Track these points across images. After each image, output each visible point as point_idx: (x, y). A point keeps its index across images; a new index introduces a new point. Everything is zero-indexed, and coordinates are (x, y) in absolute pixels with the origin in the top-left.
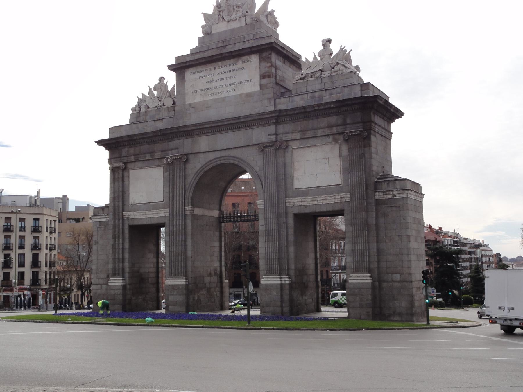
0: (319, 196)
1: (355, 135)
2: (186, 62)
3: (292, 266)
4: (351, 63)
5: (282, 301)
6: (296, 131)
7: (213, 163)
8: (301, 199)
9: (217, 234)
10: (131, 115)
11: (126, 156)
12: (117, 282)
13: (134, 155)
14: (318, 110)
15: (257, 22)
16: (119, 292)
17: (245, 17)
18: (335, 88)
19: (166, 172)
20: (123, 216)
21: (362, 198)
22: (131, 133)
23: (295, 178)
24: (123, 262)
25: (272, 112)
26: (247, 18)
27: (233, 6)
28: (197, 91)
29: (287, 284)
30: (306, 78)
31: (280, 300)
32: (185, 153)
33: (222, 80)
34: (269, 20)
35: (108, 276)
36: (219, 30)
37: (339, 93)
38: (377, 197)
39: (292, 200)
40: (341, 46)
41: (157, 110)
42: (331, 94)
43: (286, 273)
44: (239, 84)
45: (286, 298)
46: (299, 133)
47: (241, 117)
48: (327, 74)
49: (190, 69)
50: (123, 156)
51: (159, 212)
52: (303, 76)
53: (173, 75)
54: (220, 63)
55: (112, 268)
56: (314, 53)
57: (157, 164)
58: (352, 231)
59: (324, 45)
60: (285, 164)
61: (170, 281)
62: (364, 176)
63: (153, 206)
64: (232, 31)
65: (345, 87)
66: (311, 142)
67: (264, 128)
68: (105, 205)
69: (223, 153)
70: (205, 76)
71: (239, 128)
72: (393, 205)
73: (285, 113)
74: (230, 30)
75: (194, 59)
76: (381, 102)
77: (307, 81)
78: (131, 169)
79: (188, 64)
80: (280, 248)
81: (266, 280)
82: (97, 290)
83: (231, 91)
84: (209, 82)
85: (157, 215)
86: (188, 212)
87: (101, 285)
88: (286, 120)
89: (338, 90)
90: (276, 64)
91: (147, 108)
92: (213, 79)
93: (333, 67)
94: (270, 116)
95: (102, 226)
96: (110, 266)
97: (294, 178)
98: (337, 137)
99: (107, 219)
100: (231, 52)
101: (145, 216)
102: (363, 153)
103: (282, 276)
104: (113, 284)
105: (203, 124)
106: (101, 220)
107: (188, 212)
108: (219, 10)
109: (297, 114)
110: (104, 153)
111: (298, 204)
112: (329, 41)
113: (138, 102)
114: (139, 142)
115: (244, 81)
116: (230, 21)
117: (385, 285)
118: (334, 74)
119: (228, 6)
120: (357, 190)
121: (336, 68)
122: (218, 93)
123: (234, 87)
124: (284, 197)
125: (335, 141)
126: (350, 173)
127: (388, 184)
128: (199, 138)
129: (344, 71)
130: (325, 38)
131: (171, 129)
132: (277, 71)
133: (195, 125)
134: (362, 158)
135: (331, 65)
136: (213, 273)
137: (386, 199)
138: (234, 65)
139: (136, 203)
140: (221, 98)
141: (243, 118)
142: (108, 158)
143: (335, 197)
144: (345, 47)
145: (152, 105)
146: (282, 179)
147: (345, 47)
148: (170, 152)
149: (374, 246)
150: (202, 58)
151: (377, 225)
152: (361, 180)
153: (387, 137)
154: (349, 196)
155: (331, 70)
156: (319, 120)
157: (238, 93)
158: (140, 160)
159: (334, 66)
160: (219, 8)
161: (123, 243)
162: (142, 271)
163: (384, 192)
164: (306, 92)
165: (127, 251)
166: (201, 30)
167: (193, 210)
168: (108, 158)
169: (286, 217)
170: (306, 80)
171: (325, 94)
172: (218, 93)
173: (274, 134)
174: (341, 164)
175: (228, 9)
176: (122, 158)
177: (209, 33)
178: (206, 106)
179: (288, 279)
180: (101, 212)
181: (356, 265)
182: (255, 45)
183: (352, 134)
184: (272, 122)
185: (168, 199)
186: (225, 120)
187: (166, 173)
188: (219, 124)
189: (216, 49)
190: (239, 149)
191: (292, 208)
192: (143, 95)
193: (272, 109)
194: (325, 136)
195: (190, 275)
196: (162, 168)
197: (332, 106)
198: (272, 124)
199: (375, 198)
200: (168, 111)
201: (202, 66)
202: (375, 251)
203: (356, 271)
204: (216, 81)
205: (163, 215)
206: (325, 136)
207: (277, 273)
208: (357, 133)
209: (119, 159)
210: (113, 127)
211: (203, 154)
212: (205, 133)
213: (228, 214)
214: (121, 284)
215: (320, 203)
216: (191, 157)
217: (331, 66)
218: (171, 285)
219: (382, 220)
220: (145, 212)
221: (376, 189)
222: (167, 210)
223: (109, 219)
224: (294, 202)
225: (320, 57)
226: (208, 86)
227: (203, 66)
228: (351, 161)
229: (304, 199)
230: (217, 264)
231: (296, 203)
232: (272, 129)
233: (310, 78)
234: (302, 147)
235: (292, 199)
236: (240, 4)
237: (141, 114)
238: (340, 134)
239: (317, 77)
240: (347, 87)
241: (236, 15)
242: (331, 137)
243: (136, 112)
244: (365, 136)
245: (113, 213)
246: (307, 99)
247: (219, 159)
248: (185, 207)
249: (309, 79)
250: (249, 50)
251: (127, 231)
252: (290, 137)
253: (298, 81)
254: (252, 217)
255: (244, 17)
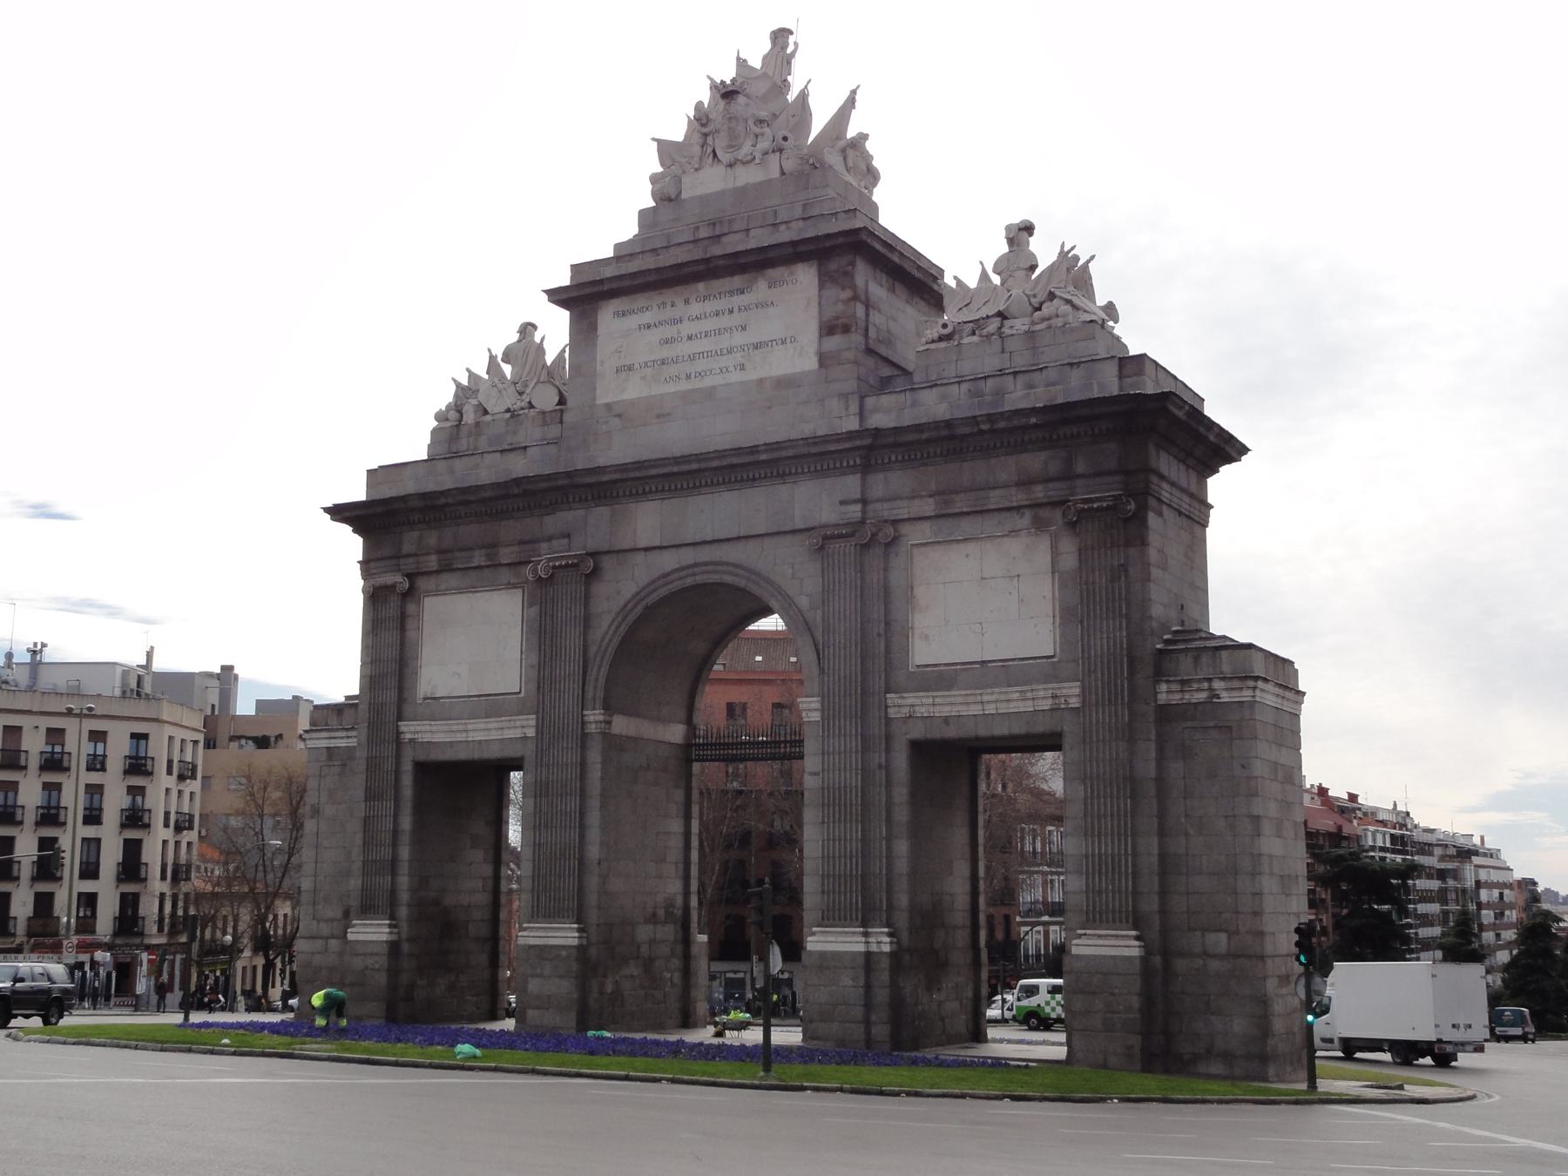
0: (989, 691)
1: (1098, 509)
2: (601, 282)
3: (903, 900)
4: (1090, 295)
5: (868, 1006)
6: (923, 493)
7: (671, 583)
8: (934, 697)
9: (679, 795)
10: (434, 432)
11: (416, 555)
12: (372, 932)
13: (439, 552)
14: (992, 431)
15: (816, 168)
16: (376, 962)
17: (781, 153)
18: (1041, 369)
19: (530, 606)
20: (399, 733)
21: (1116, 698)
22: (431, 486)
23: (917, 632)
24: (394, 872)
25: (851, 435)
26: (784, 156)
27: (746, 121)
28: (630, 368)
29: (886, 953)
30: (956, 337)
31: (862, 1003)
32: (590, 551)
34: (850, 164)
35: (347, 914)
36: (700, 191)
37: (1053, 384)
38: (1163, 698)
39: (904, 698)
40: (1063, 246)
41: (512, 420)
42: (1030, 386)
43: (881, 921)
44: (757, 348)
45: (882, 995)
46: (931, 501)
47: (761, 448)
48: (1019, 325)
49: (612, 301)
50: (404, 552)
51: (508, 724)
52: (946, 332)
53: (563, 316)
54: (701, 286)
55: (360, 888)
56: (981, 263)
57: (506, 582)
58: (1085, 799)
59: (1011, 241)
60: (887, 591)
61: (532, 934)
62: (1125, 634)
63: (490, 706)
64: (742, 191)
65: (1071, 365)
66: (967, 526)
67: (828, 482)
68: (347, 698)
69: (704, 554)
70: (657, 324)
71: (754, 479)
72: (1212, 724)
73: (891, 440)
74: (736, 190)
75: (624, 272)
76: (1180, 414)
77: (959, 344)
78: (429, 593)
79: (606, 288)
80: (865, 840)
81: (822, 939)
82: (313, 953)
84: (667, 342)
85: (500, 732)
86: (593, 726)
87: (327, 938)
88: (893, 459)
89: (1051, 374)
90: (867, 291)
91: (481, 412)
92: (679, 332)
93: (1037, 305)
94: (847, 445)
95: (336, 763)
96: (355, 883)
97: (913, 634)
98: (1045, 513)
99: (350, 740)
100: (737, 254)
101: (464, 735)
102: (1122, 565)
103: (870, 930)
104: (361, 937)
105: (646, 464)
106: (333, 743)
107: (593, 726)
108: (705, 130)
109: (928, 441)
110: (351, 544)
111: (922, 711)
112: (1028, 229)
113: (456, 396)
114: (453, 515)
115: (772, 341)
116: (735, 163)
117: (1180, 964)
118: (1038, 327)
119: (730, 118)
120: (1103, 674)
121: (1047, 309)
122: (693, 374)
123: (742, 357)
124: (883, 689)
125: (1039, 525)
126: (1081, 622)
127: (1196, 659)
128: (633, 505)
129: (1070, 319)
130: (1016, 220)
131: (549, 477)
132: (871, 312)
133: (623, 468)
134: (1120, 578)
135: (1033, 300)
136: (661, 912)
137: (1189, 704)
138: (742, 293)
139: (437, 696)
140: (701, 390)
141: (766, 451)
142: (361, 559)
143: (1035, 693)
144: (1073, 248)
145: (496, 406)
146: (879, 635)
147: (1073, 248)
148: (544, 546)
149: (1150, 846)
150: (649, 270)
151: (1160, 781)
152: (1115, 642)
153: (1197, 519)
154: (1077, 691)
155: (1033, 313)
156: (993, 461)
157: (752, 375)
158: (455, 566)
159: (1041, 304)
160: (703, 125)
161: (396, 816)
162: (449, 901)
163: (1183, 682)
164: (957, 377)
165: (405, 838)
166: (649, 187)
167: (609, 723)
168: (361, 559)
169: (888, 751)
170: (956, 343)
171: (1013, 387)
172: (693, 374)
173: (855, 502)
174: (1057, 595)
175: (730, 128)
176: (402, 561)
177: (673, 197)
178: (658, 411)
179: (888, 940)
180: (334, 722)
181: (1094, 901)
182: (810, 234)
183: (1090, 505)
184: (852, 463)
185: (533, 686)
186: (712, 455)
187: (532, 609)
188: (694, 466)
189: (691, 246)
190: (751, 542)
191: (905, 722)
192: (471, 375)
193: (852, 424)
194: (1009, 509)
195: (593, 916)
196: (519, 592)
197: (1033, 420)
198: (851, 470)
199: (1156, 700)
200: (545, 424)
201: (646, 295)
202: (1155, 860)
203: (1094, 921)
204: (690, 338)
205: (518, 733)
206: (1009, 509)
207: (857, 919)
208: (1105, 505)
209: (394, 562)
210: (380, 467)
211: (642, 554)
212: (650, 492)
213: (712, 737)
214: (385, 939)
215: (991, 709)
216: (607, 563)
217: (1030, 304)
218: (536, 946)
219: (1176, 768)
220: (466, 724)
221: (1159, 674)
222: (531, 720)
223: (355, 740)
224: (913, 706)
225: (998, 274)
226: (666, 352)
227: (651, 293)
228: (1085, 586)
229: (941, 696)
230: (674, 887)
231: (917, 709)
232: (850, 485)
233: (967, 336)
234: (939, 542)
235: (905, 695)
236: (766, 114)
237: (464, 431)
238: (1053, 504)
239: (989, 336)
240: (1078, 367)
241: (754, 146)
242: (1028, 515)
243: (448, 424)
244: (1130, 514)
245: (369, 723)
246: (959, 399)
247: (691, 571)
248: (585, 713)
249: (965, 341)
250: (790, 250)
251: (407, 780)
252: (906, 511)
253: (933, 346)
254: (785, 747)
255: (778, 153)
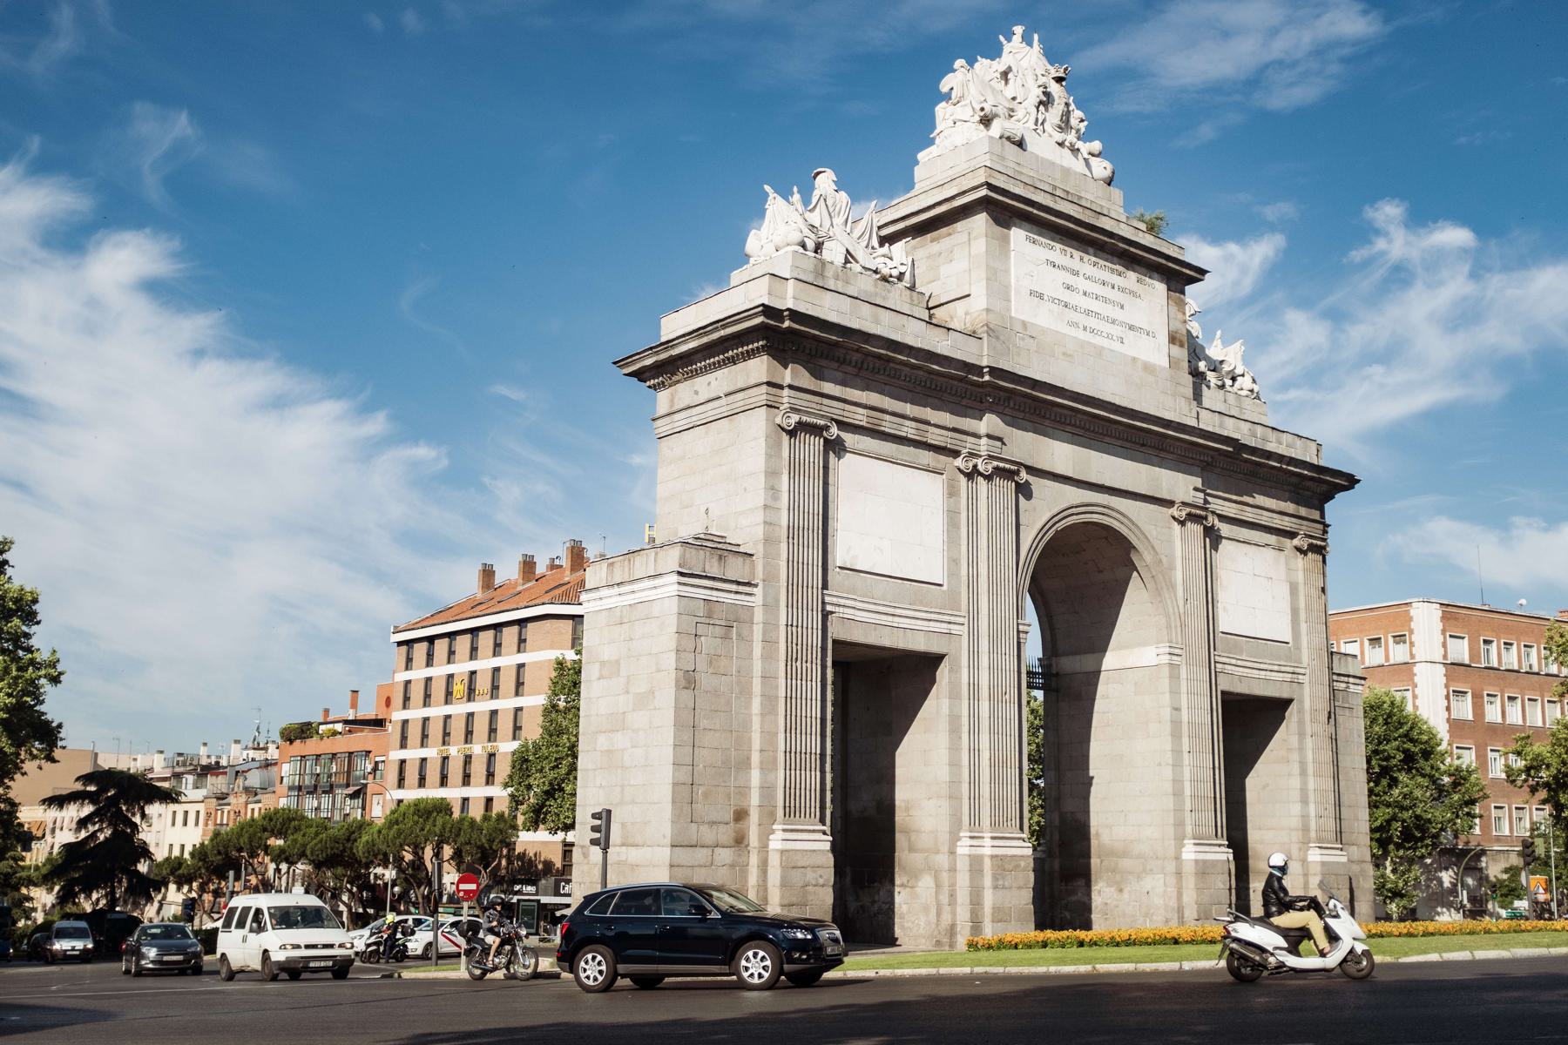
16: (821, 876)
28: (1041, 296)
33: (1096, 298)
83: (1115, 338)
84: (1068, 288)
106: (715, 595)
140: (1095, 346)
226: (1066, 296)
